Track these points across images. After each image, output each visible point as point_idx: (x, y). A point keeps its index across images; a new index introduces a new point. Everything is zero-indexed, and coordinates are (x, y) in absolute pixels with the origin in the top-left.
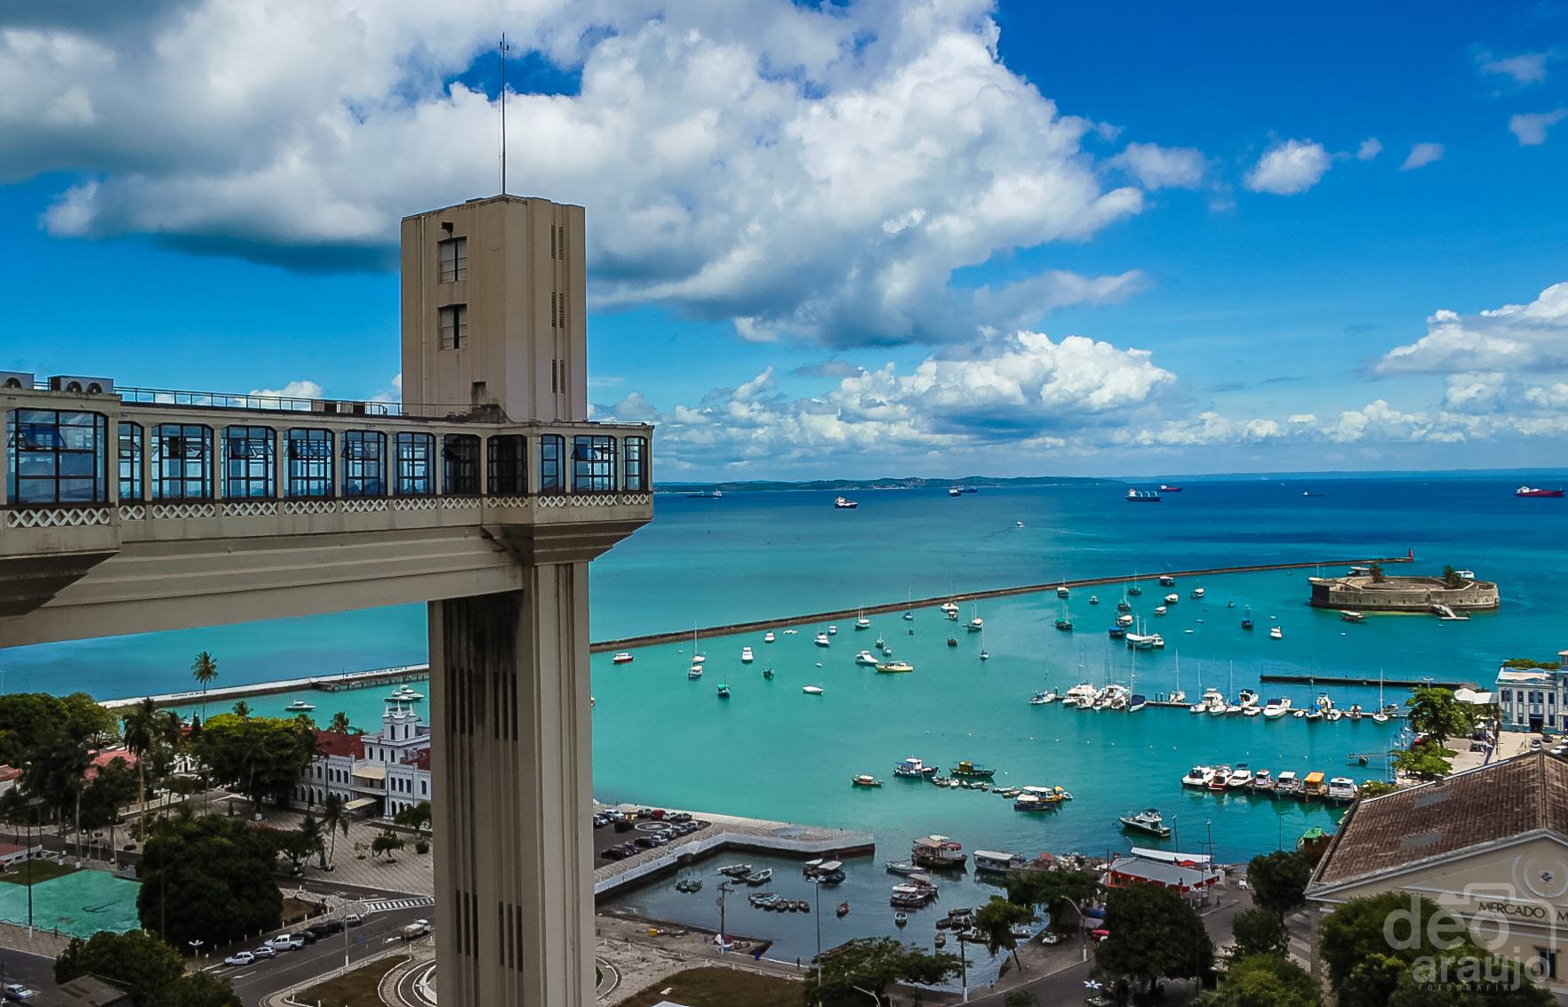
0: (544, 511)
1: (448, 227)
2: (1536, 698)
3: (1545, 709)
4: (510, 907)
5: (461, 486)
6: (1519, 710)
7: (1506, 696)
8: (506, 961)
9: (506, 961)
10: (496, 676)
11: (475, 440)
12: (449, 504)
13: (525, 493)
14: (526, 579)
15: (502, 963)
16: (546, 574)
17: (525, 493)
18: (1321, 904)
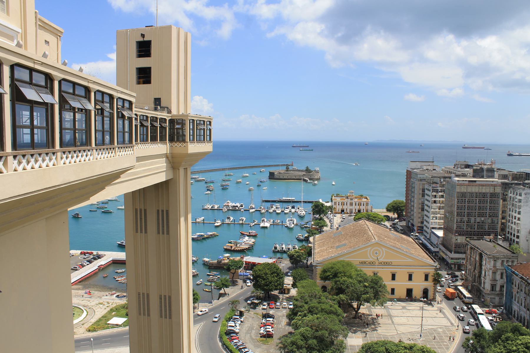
0: (194, 148)
1: (143, 36)
2: (343, 204)
3: (345, 207)
4: (165, 296)
5: (163, 139)
6: (339, 208)
7: (335, 203)
8: (168, 317)
9: (168, 317)
10: (158, 211)
11: (165, 119)
12: (159, 145)
13: (184, 141)
14: (174, 174)
15: (161, 316)
16: (182, 171)
17: (184, 141)
18: (317, 266)
